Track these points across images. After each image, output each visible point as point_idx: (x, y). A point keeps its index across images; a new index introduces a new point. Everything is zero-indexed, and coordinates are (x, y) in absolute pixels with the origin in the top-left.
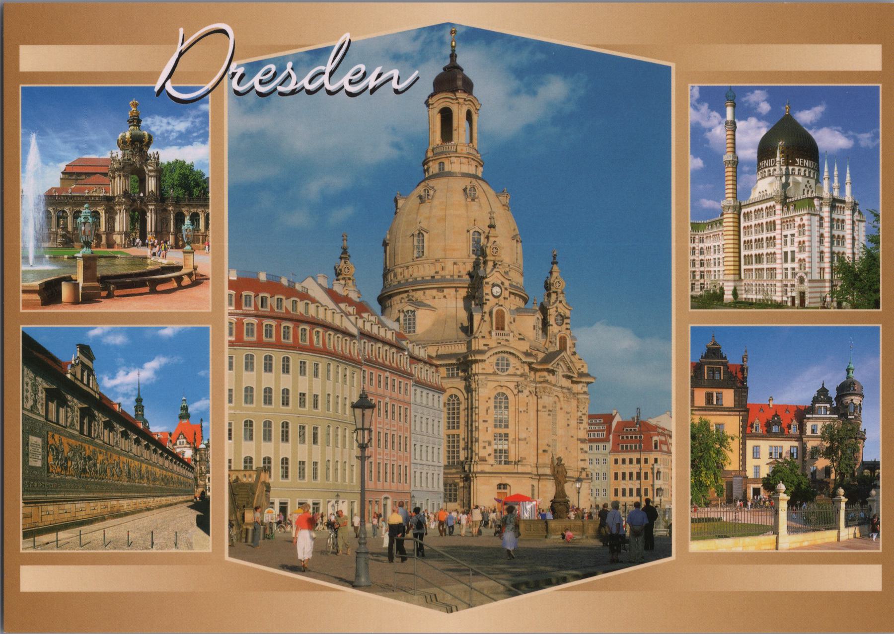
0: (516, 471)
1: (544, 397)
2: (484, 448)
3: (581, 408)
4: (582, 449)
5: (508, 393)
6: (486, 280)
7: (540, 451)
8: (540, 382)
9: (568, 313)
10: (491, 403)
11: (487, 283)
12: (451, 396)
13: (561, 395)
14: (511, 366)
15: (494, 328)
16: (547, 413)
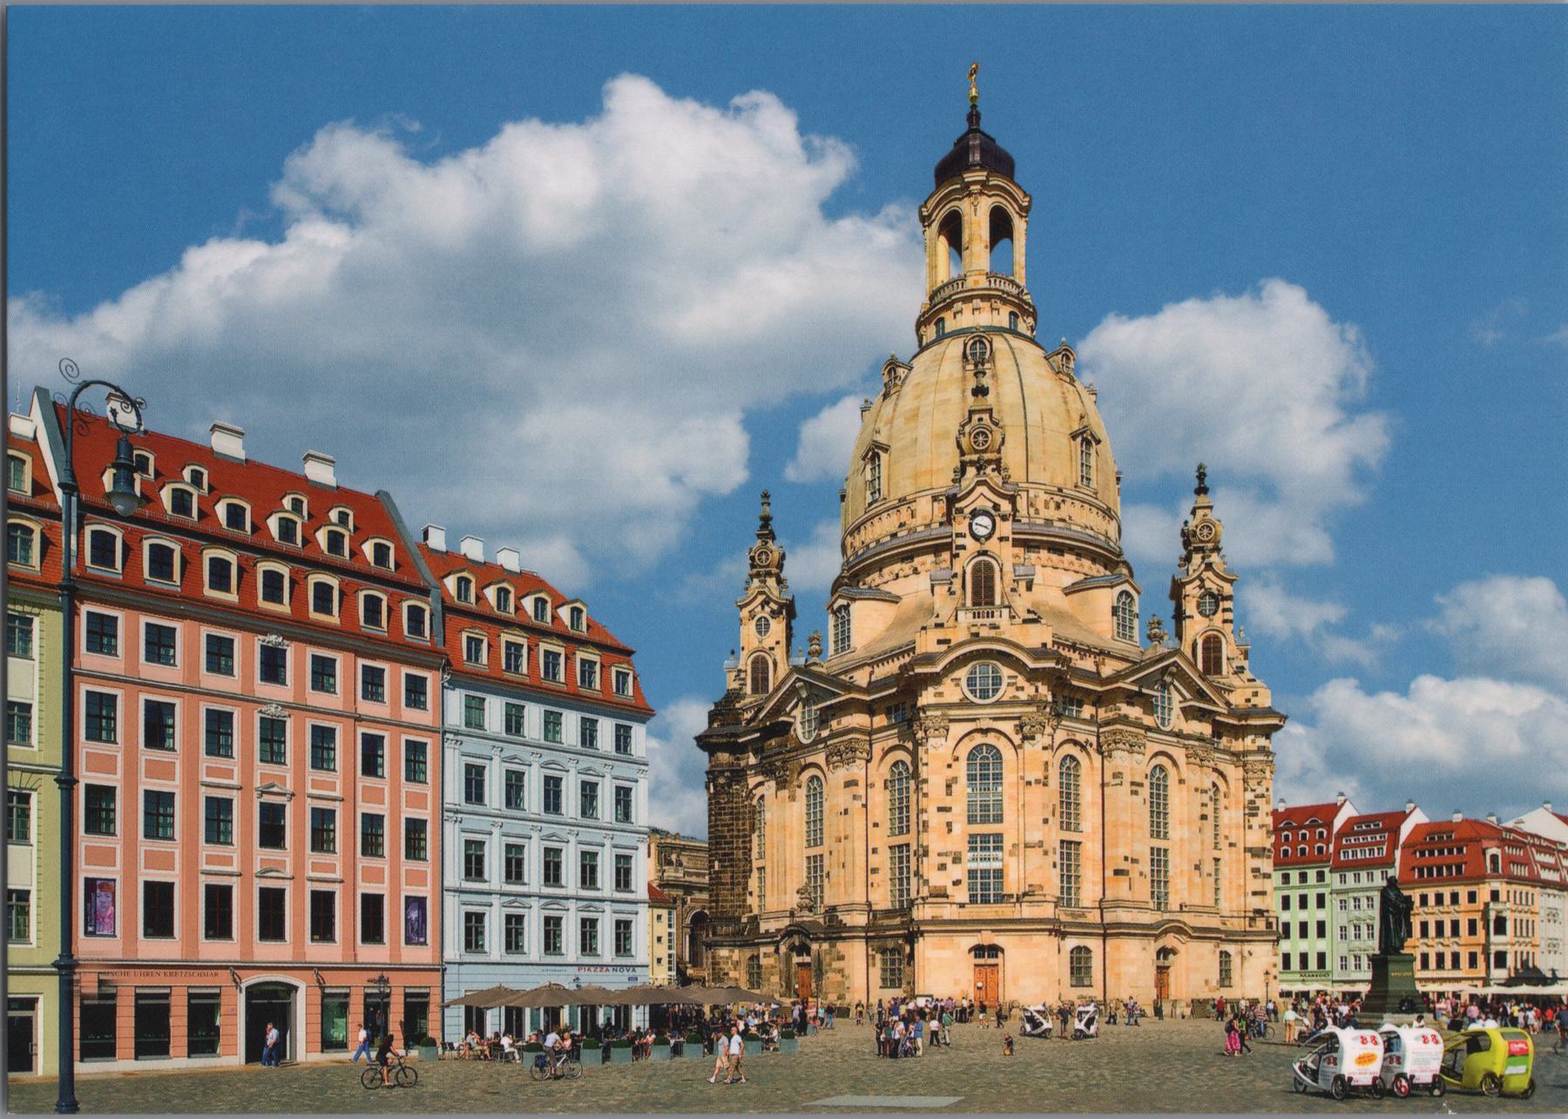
0: (1017, 916)
1: (1115, 753)
2: (942, 867)
3: (1253, 784)
4: (1256, 870)
5: (1002, 744)
6: (958, 505)
7: (1109, 873)
8: (1107, 723)
9: (1228, 589)
10: (961, 770)
11: (960, 511)
12: (896, 764)
13: (1179, 754)
14: (1005, 681)
15: (969, 603)
16: (1127, 788)
